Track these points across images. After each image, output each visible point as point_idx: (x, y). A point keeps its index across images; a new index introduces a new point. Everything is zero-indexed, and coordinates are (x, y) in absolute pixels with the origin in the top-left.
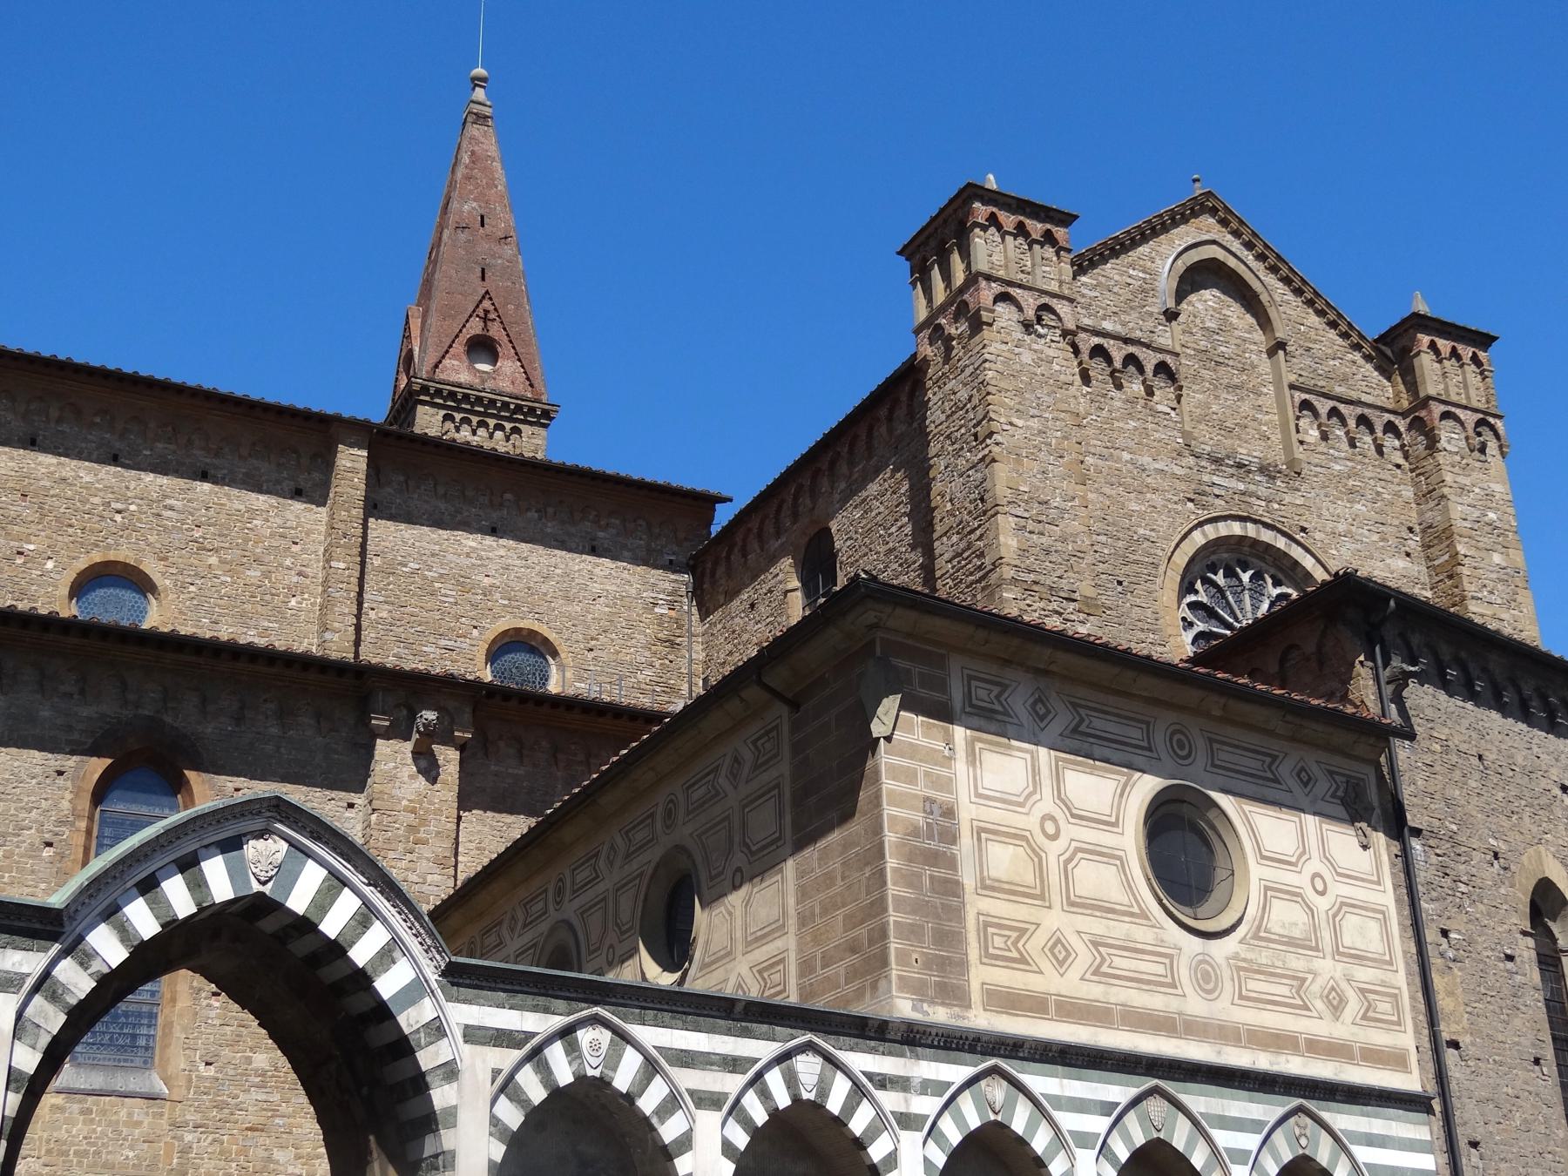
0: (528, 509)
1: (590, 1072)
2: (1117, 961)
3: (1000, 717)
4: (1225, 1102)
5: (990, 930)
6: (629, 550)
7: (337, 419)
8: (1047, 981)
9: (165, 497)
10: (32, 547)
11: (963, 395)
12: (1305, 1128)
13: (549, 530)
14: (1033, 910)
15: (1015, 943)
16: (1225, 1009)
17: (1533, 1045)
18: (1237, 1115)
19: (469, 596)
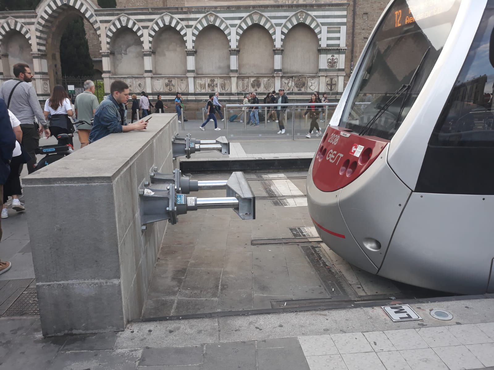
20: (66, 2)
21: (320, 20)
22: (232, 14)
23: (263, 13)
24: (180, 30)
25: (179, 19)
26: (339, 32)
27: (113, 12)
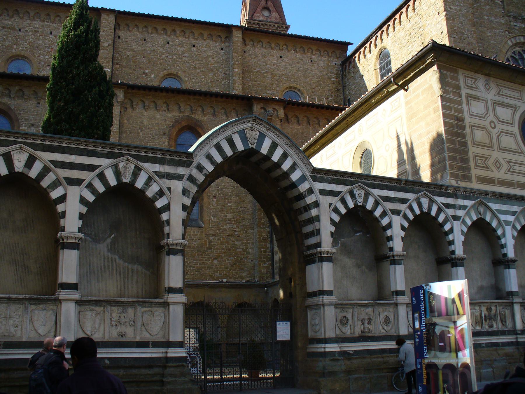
0: (291, 50)
1: (359, 204)
2: (515, 168)
3: (475, 89)
5: (477, 158)
6: (322, 61)
7: (232, 26)
8: (495, 174)
9: (184, 53)
10: (147, 71)
13: (298, 56)
14: (489, 151)
19: (275, 77)
20: (255, 145)
24: (443, 222)
27: (342, 178)
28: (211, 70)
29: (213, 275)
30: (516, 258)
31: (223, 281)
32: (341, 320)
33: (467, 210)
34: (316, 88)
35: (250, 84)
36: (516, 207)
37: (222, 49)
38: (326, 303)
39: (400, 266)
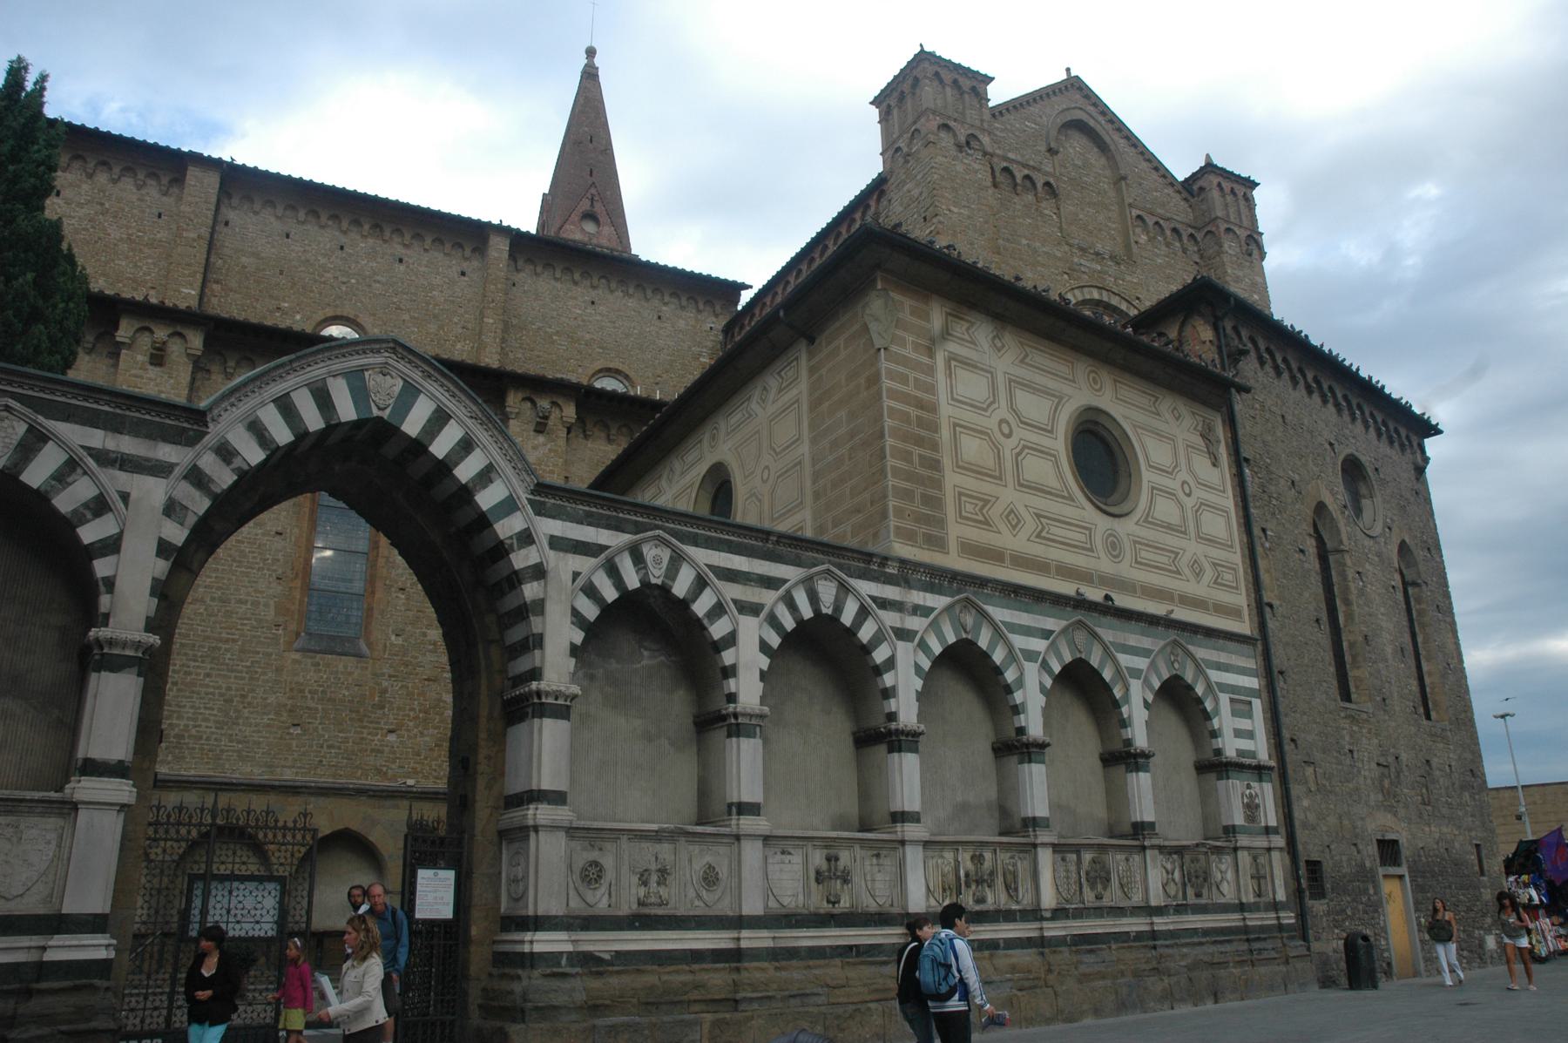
1: (654, 581)
2: (1053, 530)
4: (1127, 634)
5: (963, 498)
10: (286, 305)
11: (916, 192)
12: (1177, 656)
15: (981, 509)
16: (1127, 570)
17: (1316, 610)
18: (1134, 644)
20: (388, 411)
21: (1215, 676)
22: (1025, 615)
23: (1099, 630)
25: (872, 597)
26: (1249, 715)
28: (435, 316)
29: (384, 769)
30: (1047, 740)
31: (405, 783)
32: (584, 869)
33: (932, 616)
34: (664, 376)
35: (520, 356)
36: (1052, 620)
37: (463, 274)
38: (543, 822)
39: (752, 740)
